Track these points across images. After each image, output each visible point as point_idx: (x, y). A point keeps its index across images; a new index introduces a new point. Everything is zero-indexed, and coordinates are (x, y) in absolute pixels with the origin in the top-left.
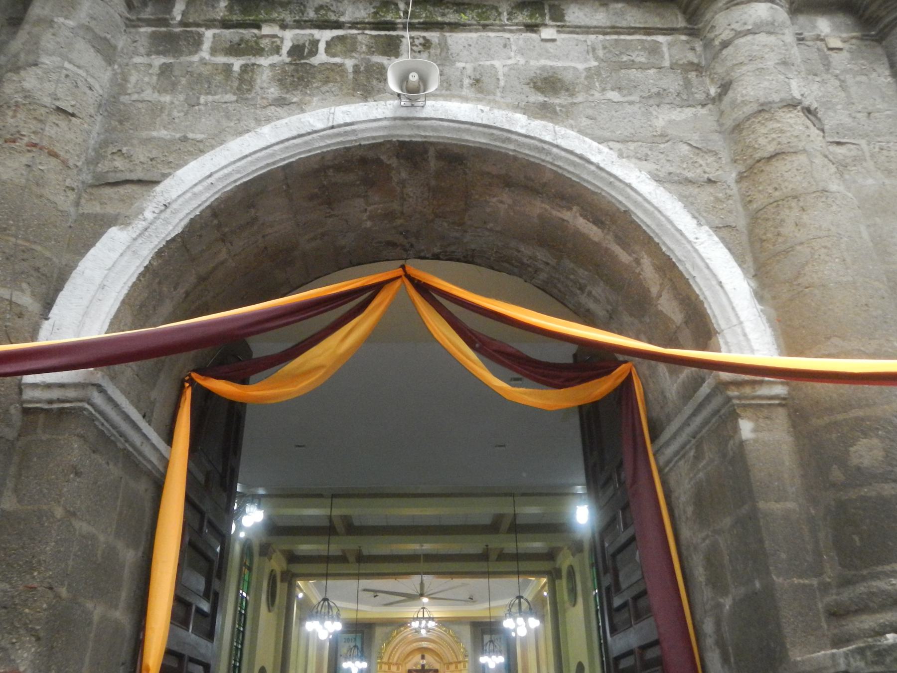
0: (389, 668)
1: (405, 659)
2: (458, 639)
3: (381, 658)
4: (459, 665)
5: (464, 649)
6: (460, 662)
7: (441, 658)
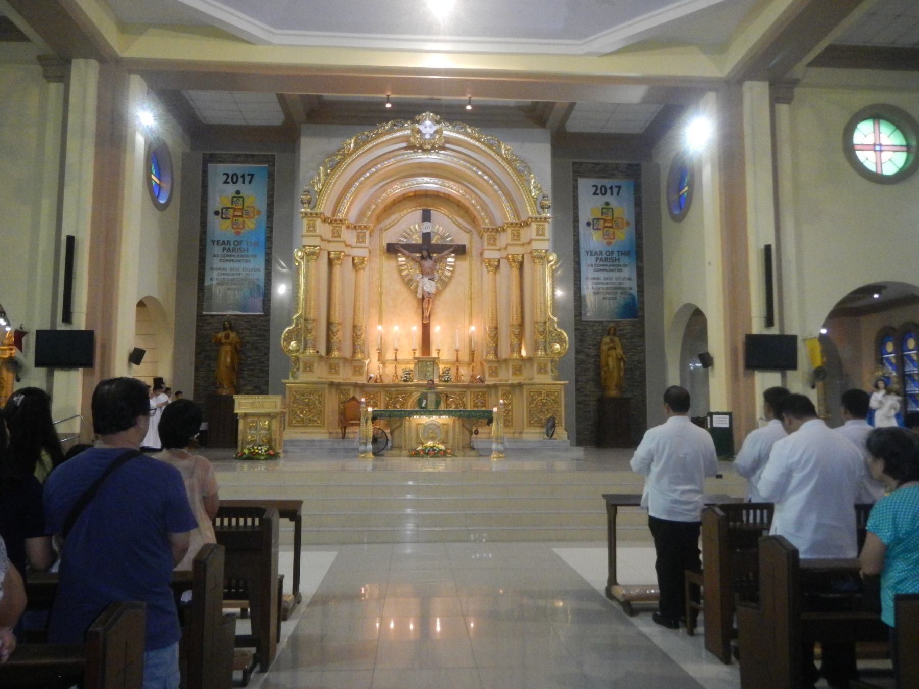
0: (336, 234)
1: (379, 219)
2: (522, 170)
3: (313, 208)
4: (523, 231)
5: (540, 189)
6: (527, 224)
7: (473, 220)
